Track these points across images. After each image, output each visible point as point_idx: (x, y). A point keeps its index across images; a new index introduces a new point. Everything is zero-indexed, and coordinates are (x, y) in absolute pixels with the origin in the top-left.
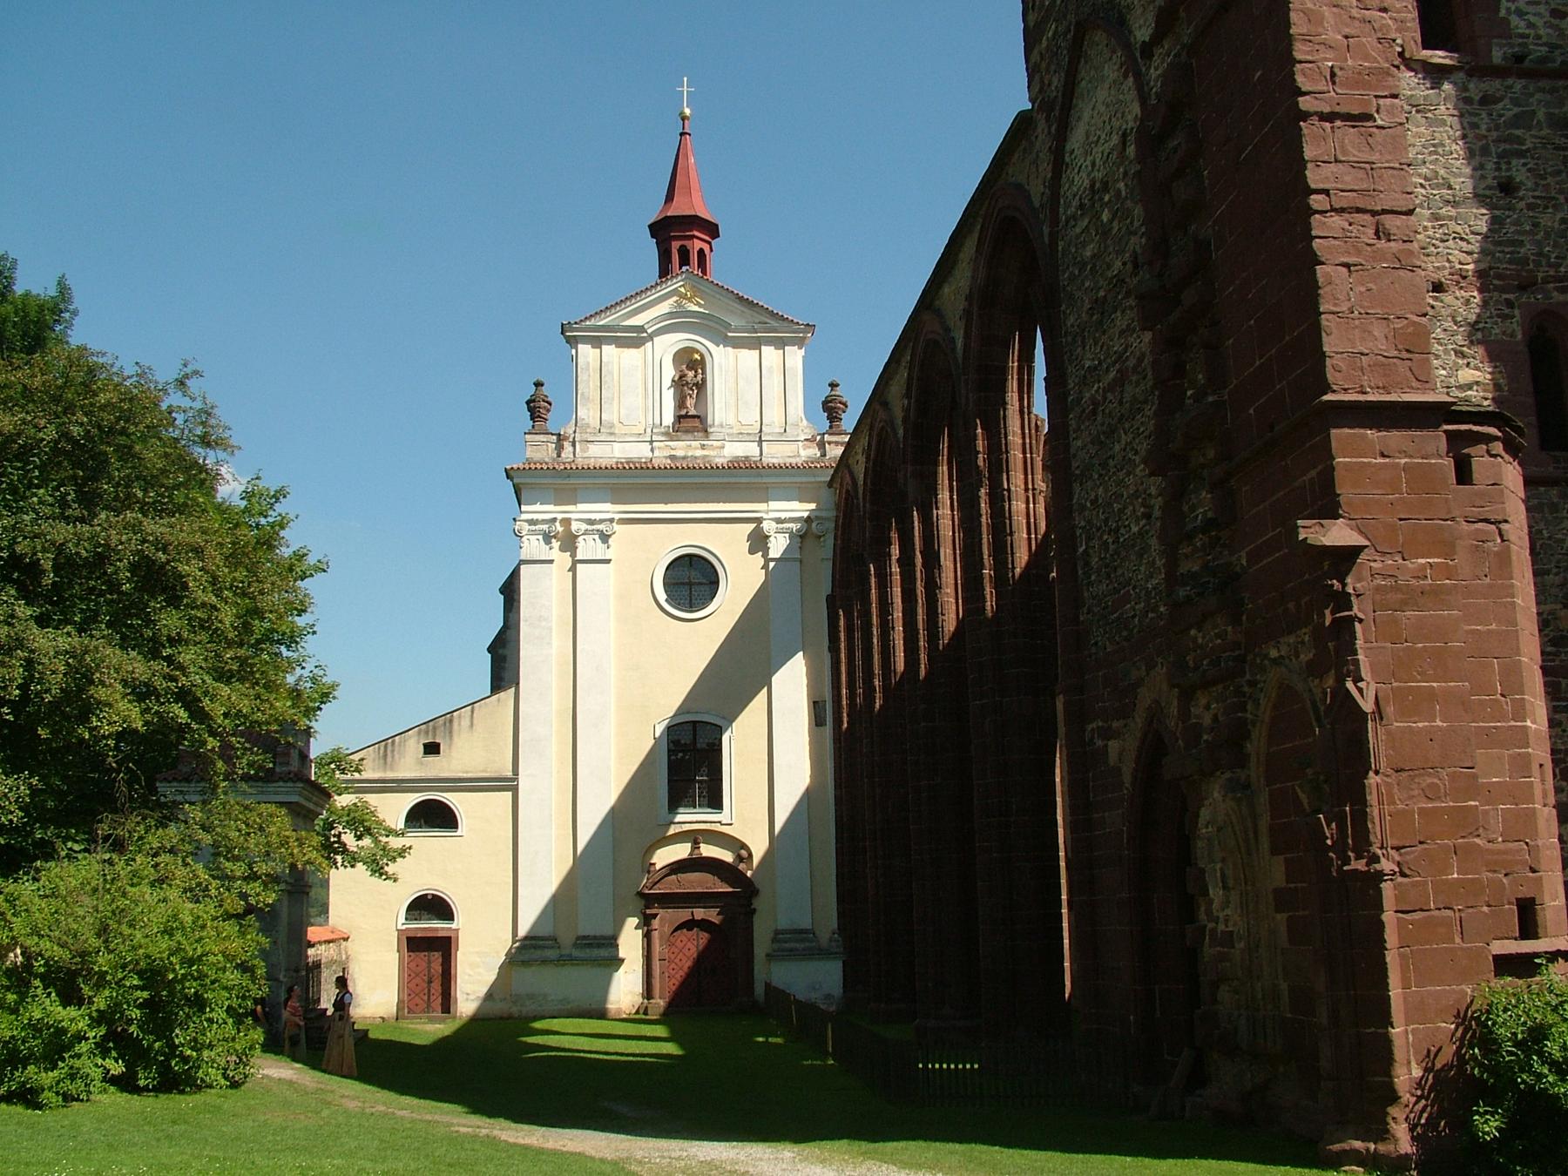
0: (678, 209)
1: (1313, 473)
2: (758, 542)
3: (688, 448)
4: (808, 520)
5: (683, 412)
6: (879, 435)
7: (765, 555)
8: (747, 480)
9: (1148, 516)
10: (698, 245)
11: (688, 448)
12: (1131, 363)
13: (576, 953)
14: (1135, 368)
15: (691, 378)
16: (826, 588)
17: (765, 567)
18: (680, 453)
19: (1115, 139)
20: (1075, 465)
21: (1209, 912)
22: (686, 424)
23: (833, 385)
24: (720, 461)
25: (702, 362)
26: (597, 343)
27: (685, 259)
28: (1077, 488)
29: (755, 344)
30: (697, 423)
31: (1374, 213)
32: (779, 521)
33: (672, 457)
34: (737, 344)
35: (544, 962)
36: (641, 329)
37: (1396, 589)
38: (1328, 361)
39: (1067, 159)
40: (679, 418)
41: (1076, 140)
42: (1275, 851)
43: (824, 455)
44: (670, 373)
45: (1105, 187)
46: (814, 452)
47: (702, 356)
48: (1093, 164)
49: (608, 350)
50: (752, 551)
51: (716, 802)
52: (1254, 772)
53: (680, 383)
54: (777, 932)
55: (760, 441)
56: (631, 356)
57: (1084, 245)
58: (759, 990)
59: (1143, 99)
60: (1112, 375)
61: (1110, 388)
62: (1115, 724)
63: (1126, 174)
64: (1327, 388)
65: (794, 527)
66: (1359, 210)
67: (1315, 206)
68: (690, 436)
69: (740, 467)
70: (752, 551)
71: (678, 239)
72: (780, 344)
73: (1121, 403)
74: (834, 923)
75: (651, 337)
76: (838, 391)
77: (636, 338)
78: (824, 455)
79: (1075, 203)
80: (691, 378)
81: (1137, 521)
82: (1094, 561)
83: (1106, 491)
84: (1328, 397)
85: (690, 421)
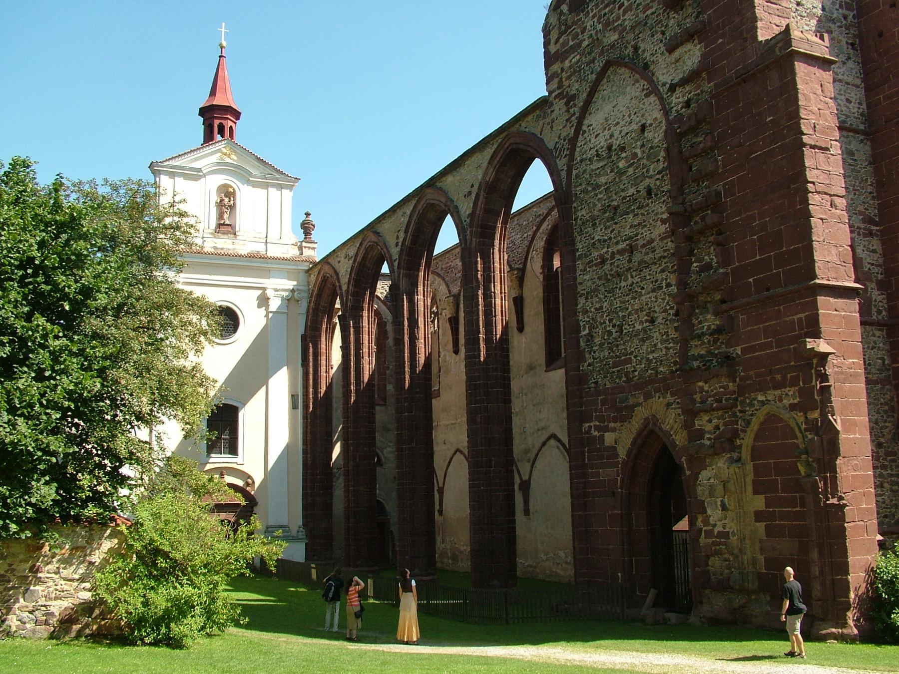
0: (218, 101)
1: (802, 315)
2: (263, 301)
3: (224, 243)
4: (293, 291)
5: (222, 222)
6: (366, 249)
7: (267, 309)
8: (256, 264)
9: (652, 321)
10: (230, 123)
11: (224, 243)
12: (641, 242)
14: (643, 246)
15: (226, 202)
16: (301, 330)
17: (267, 316)
19: (634, 126)
20: (580, 288)
21: (706, 522)
22: (223, 229)
23: (308, 214)
25: (234, 193)
26: (172, 175)
27: (221, 131)
28: (582, 301)
29: (266, 186)
30: (229, 229)
31: (831, 195)
32: (276, 290)
33: (215, 248)
34: (254, 185)
36: (200, 170)
37: (842, 373)
38: (816, 264)
39: (585, 128)
40: (219, 225)
41: (595, 120)
42: (756, 492)
44: (215, 198)
45: (622, 149)
47: (234, 189)
48: (612, 136)
49: (179, 180)
50: (259, 306)
52: (746, 454)
53: (220, 205)
55: (266, 242)
57: (599, 175)
59: (666, 112)
60: (621, 246)
61: (621, 252)
62: (612, 425)
63: (643, 146)
64: (815, 276)
65: (285, 294)
66: (826, 193)
67: (810, 189)
68: (225, 236)
70: (259, 306)
71: (216, 119)
72: (280, 187)
73: (630, 261)
74: (300, 522)
75: (204, 176)
76: (310, 218)
77: (195, 175)
78: (302, 254)
79: (593, 152)
80: (226, 202)
81: (642, 323)
82: (597, 340)
83: (611, 305)
84: (817, 281)
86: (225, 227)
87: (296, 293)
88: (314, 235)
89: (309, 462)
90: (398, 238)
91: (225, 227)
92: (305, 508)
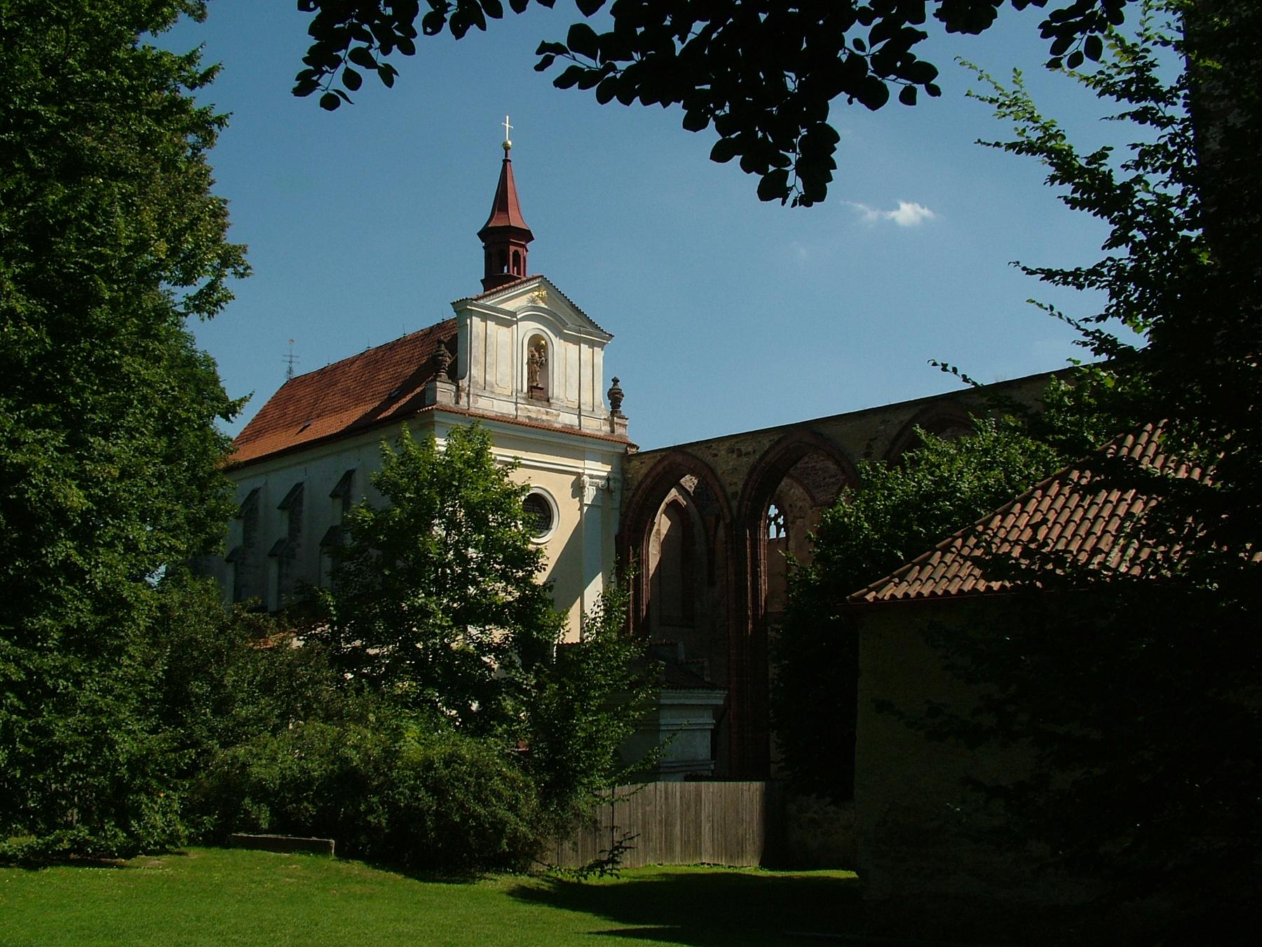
2: (578, 489)
3: (535, 412)
4: (608, 479)
7: (581, 501)
8: (569, 441)
11: (535, 412)
17: (581, 509)
18: (533, 415)
22: (537, 393)
24: (557, 426)
25: (545, 347)
26: (485, 318)
29: (577, 341)
32: (591, 477)
33: (529, 417)
34: (567, 338)
36: (513, 314)
40: (531, 388)
43: (613, 431)
46: (607, 428)
50: (574, 497)
53: (531, 361)
55: (579, 415)
65: (601, 483)
69: (567, 432)
70: (574, 497)
72: (592, 344)
77: (508, 320)
78: (613, 431)
86: (538, 391)
88: (624, 407)
91: (538, 391)
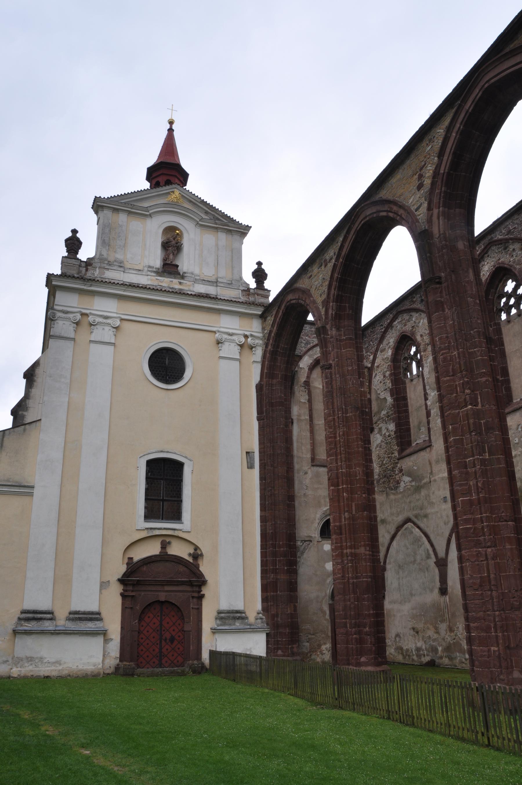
13: (72, 626)
15: (172, 244)
25: (180, 235)
35: (43, 633)
36: (147, 209)
47: (181, 232)
49: (122, 218)
51: (176, 515)
53: (165, 246)
54: (219, 612)
56: (135, 225)
58: (205, 656)
74: (259, 606)
75: (150, 216)
80: (172, 244)
85: (169, 268)
87: (249, 339)
89: (269, 531)
90: (421, 176)
92: (264, 588)
